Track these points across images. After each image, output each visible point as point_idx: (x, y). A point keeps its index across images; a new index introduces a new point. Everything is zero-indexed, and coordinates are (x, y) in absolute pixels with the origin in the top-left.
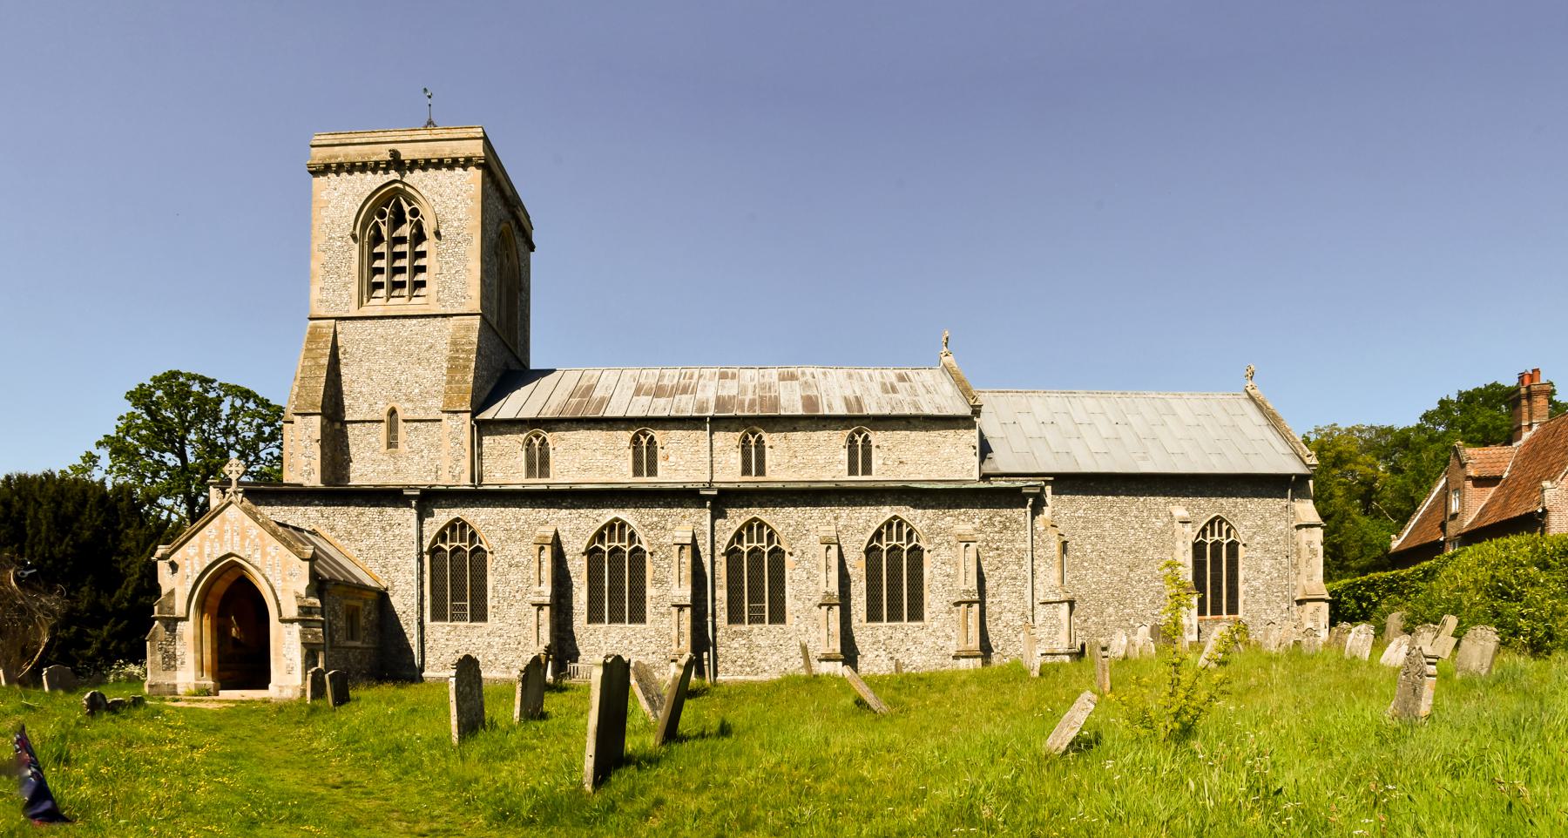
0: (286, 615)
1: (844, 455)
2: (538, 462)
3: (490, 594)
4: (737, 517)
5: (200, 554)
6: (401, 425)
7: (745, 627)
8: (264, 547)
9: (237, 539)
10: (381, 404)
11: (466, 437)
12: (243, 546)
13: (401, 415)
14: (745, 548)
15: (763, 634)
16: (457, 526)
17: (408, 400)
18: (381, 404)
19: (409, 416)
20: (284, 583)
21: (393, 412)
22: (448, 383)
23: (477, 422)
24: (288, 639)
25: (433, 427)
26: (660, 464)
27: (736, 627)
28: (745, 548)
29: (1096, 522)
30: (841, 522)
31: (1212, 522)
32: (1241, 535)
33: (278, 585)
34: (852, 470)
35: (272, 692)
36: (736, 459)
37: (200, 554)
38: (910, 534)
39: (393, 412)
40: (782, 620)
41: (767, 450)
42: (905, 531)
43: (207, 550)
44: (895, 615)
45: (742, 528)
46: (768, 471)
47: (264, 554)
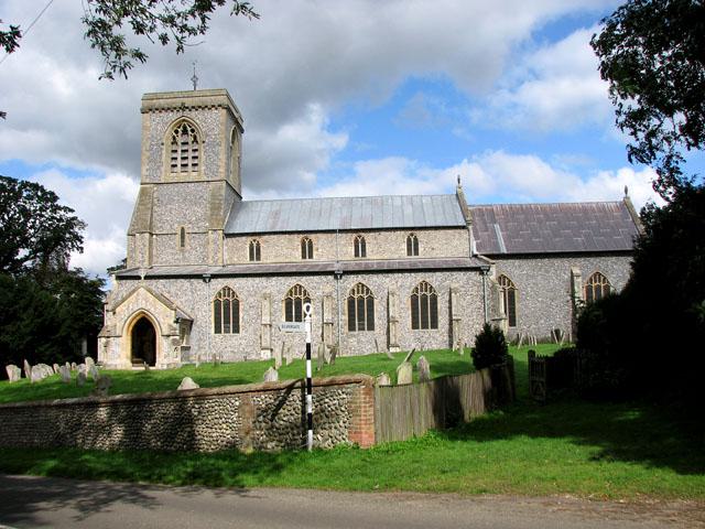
1: (405, 246)
3: (241, 320)
6: (186, 235)
7: (356, 332)
10: (176, 225)
13: (187, 230)
15: (366, 335)
16: (227, 289)
18: (176, 225)
20: (164, 321)
21: (183, 229)
25: (202, 237)
26: (315, 253)
29: (533, 277)
30: (399, 284)
31: (595, 275)
36: (352, 250)
39: (183, 229)
40: (373, 329)
44: (425, 326)
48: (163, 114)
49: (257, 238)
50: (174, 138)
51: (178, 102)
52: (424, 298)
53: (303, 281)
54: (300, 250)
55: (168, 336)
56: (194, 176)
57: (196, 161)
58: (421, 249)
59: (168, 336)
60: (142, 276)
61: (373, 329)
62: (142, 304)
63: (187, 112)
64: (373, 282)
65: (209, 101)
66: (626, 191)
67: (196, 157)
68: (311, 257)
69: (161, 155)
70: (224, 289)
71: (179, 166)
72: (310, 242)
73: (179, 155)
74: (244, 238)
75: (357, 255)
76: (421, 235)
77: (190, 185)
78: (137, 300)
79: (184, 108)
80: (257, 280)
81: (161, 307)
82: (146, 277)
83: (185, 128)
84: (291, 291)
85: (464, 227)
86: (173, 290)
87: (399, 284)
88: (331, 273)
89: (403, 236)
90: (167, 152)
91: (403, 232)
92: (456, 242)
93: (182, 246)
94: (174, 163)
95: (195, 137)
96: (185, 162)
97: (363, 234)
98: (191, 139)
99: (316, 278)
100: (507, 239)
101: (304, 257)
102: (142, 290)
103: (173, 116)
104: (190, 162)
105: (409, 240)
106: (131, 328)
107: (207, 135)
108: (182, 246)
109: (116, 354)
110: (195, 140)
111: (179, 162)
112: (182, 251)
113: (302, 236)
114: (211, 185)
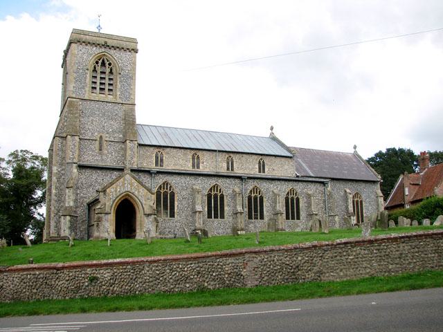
1: (257, 166)
3: (176, 208)
4: (250, 185)
6: (104, 144)
7: (253, 221)
11: (135, 150)
13: (104, 138)
14: (253, 195)
19: (107, 139)
21: (101, 137)
28: (253, 195)
32: (363, 197)
33: (144, 202)
34: (260, 172)
36: (225, 165)
37: (116, 191)
38: (170, 187)
39: (101, 137)
40: (263, 219)
47: (139, 192)
48: (89, 47)
49: (161, 150)
50: (95, 67)
51: (102, 41)
52: (292, 199)
53: (220, 182)
55: (148, 215)
56: (110, 98)
57: (111, 88)
59: (148, 215)
61: (263, 219)
62: (128, 188)
63: (107, 49)
64: (264, 186)
65: (124, 44)
66: (355, 147)
67: (112, 85)
69: (86, 78)
71: (98, 88)
73: (98, 81)
74: (152, 149)
75: (228, 169)
76: (266, 160)
77: (108, 104)
79: (106, 45)
80: (188, 178)
81: (143, 191)
83: (103, 61)
84: (211, 189)
85: (291, 157)
89: (256, 159)
91: (256, 157)
92: (286, 167)
93: (100, 150)
95: (111, 70)
96: (102, 87)
98: (108, 70)
99: (228, 180)
100: (310, 168)
104: (107, 87)
105: (260, 162)
107: (122, 69)
108: (100, 150)
110: (111, 72)
111: (98, 86)
112: (100, 154)
113: (193, 152)
114: (124, 107)
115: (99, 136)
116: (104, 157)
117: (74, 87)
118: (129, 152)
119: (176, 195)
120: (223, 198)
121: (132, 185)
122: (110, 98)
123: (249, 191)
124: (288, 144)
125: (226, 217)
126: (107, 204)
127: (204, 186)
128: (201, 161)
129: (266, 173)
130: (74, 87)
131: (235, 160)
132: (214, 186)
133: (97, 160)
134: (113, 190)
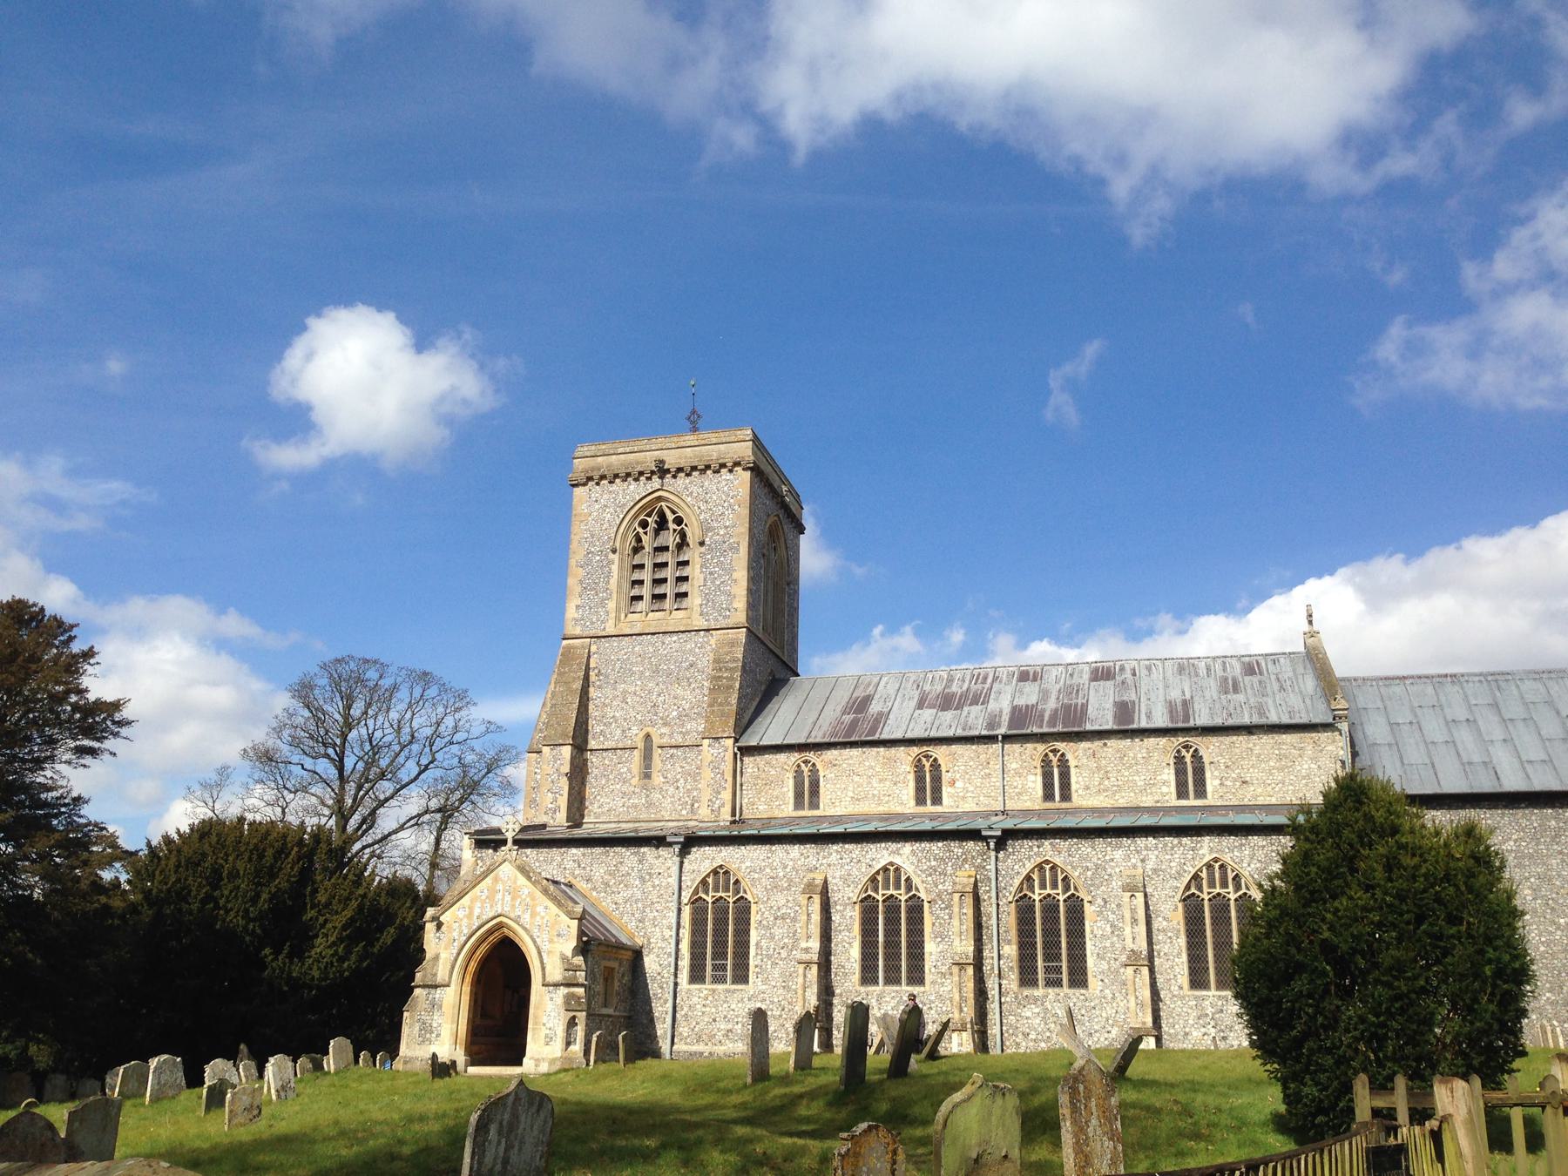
0: (549, 979)
1: (1169, 775)
2: (807, 791)
4: (1023, 858)
5: (470, 916)
6: (657, 752)
7: (1039, 992)
8: (534, 906)
9: (508, 898)
10: (635, 730)
12: (513, 906)
13: (656, 741)
17: (665, 724)
18: (635, 730)
19: (665, 741)
21: (648, 736)
22: (711, 705)
23: (740, 749)
24: (549, 1006)
25: (691, 754)
26: (946, 791)
27: (1027, 992)
30: (1150, 865)
33: (545, 947)
35: (529, 1066)
36: (1035, 783)
37: (470, 916)
39: (648, 736)
41: (1073, 771)
42: (1231, 876)
43: (477, 911)
45: (1032, 871)
46: (1074, 796)
47: (533, 915)
49: (811, 756)
53: (905, 856)
54: (912, 785)
58: (1211, 784)
60: (510, 836)
68: (937, 800)
70: (715, 872)
72: (936, 766)
73: (646, 575)
74: (782, 757)
75: (1048, 795)
76: (1209, 748)
77: (668, 639)
78: (493, 891)
80: (795, 850)
81: (547, 911)
82: (521, 843)
83: (662, 515)
84: (873, 879)
86: (599, 872)
87: (1150, 865)
88: (974, 835)
90: (621, 568)
91: (1163, 741)
94: (636, 592)
95: (683, 535)
96: (659, 591)
97: (1061, 746)
98: (670, 539)
101: (920, 800)
102: (507, 870)
103: (635, 491)
105: (1179, 760)
106: (473, 966)
107: (709, 529)
108: (647, 776)
109: (437, 1024)
110: (683, 544)
111: (646, 591)
113: (915, 750)
115: (642, 734)
116: (656, 796)
117: (578, 607)
118: (707, 774)
119: (754, 908)
120: (747, 910)
121: (514, 893)
122: (677, 619)
123: (1017, 882)
124: (1340, 670)
125: (928, 977)
126: (443, 956)
127: (845, 870)
128: (945, 777)
129: (1212, 799)
130: (578, 607)
131: (1072, 763)
132: (885, 869)
133: (635, 806)
134: (461, 914)
